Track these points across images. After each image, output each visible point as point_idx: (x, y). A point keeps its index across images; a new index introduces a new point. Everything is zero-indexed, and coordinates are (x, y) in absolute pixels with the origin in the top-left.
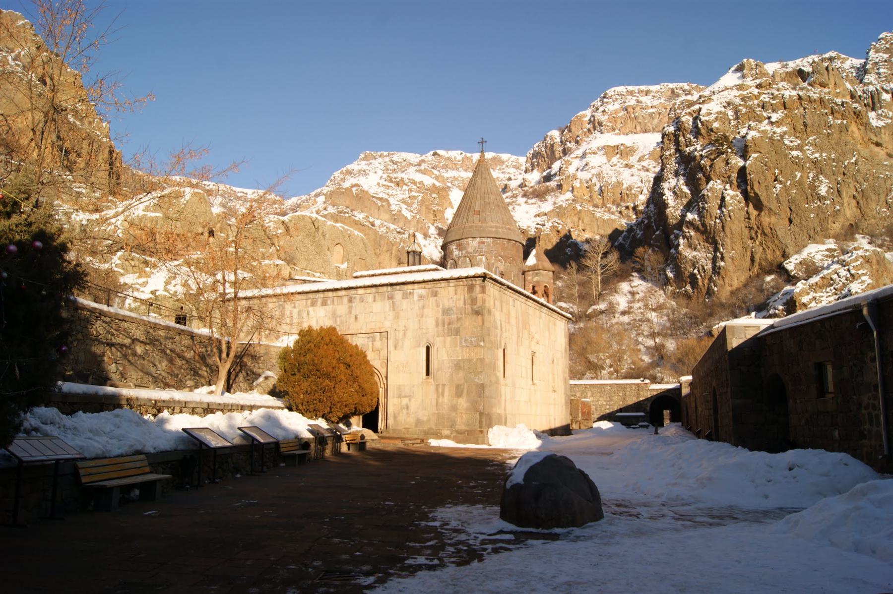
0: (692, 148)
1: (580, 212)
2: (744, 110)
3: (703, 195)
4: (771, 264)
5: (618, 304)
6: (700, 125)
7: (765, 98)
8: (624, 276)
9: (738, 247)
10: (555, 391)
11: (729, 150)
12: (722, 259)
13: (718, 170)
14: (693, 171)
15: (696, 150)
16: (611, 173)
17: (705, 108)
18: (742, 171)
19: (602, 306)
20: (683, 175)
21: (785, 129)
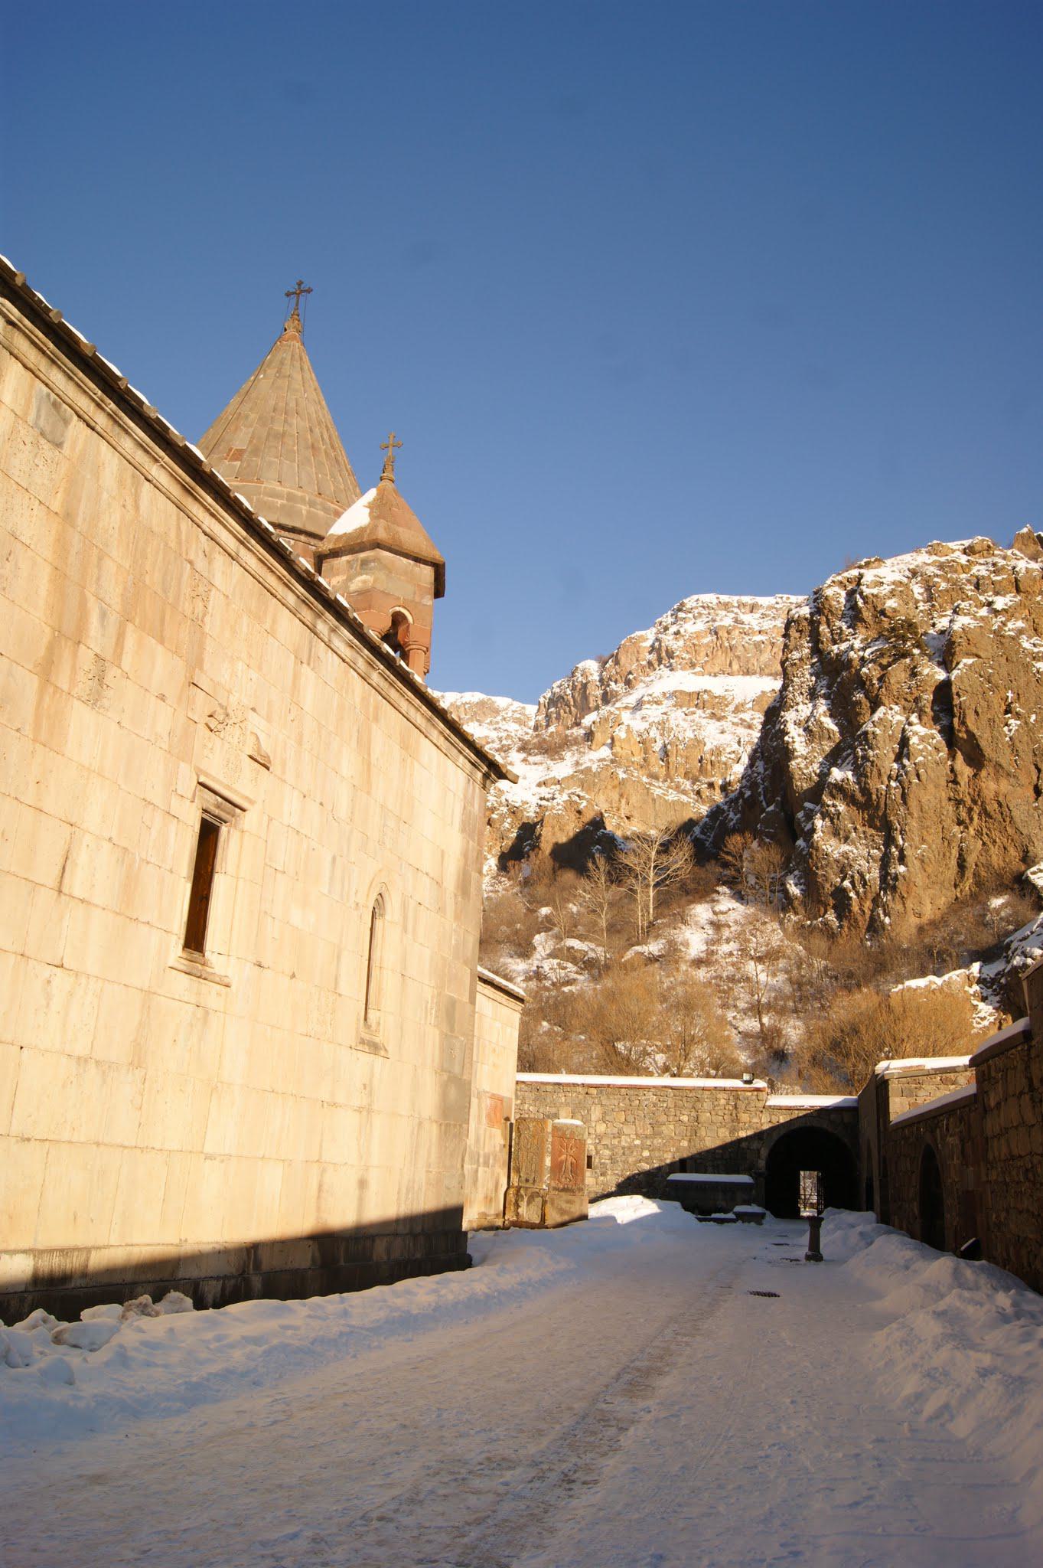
0: (844, 646)
1: (623, 783)
2: (944, 585)
3: (866, 733)
4: (999, 876)
5: (686, 944)
6: (860, 602)
7: (981, 570)
8: (703, 892)
9: (934, 838)
10: (375, 1048)
11: (916, 651)
12: (902, 859)
13: (895, 688)
14: (844, 688)
15: (852, 648)
16: (685, 725)
17: (869, 575)
18: (943, 691)
19: (654, 947)
20: (826, 697)
21: (1020, 624)
